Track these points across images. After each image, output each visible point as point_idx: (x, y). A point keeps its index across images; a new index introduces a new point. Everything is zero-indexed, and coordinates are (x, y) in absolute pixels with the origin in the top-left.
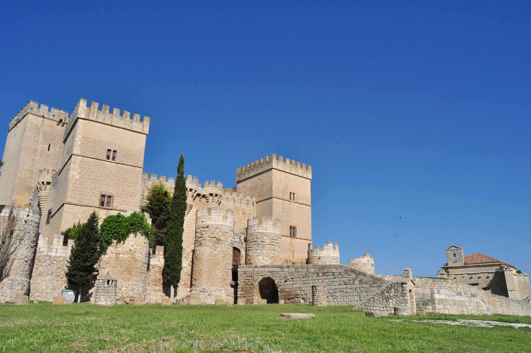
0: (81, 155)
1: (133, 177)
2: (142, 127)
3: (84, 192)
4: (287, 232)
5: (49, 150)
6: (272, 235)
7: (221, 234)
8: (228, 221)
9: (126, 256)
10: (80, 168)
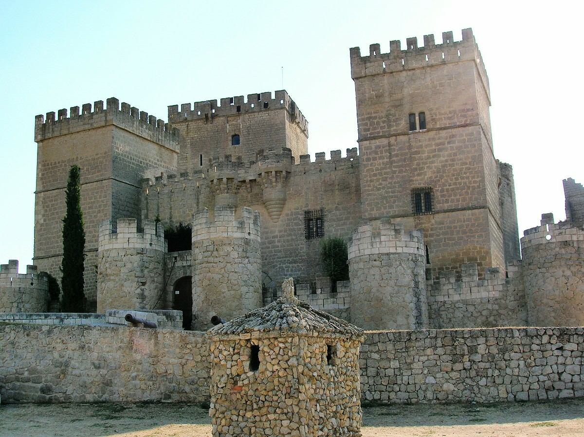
0: (44, 189)
1: (100, 196)
2: (104, 118)
3: (49, 238)
5: (201, 165)
7: (107, 265)
10: (44, 207)
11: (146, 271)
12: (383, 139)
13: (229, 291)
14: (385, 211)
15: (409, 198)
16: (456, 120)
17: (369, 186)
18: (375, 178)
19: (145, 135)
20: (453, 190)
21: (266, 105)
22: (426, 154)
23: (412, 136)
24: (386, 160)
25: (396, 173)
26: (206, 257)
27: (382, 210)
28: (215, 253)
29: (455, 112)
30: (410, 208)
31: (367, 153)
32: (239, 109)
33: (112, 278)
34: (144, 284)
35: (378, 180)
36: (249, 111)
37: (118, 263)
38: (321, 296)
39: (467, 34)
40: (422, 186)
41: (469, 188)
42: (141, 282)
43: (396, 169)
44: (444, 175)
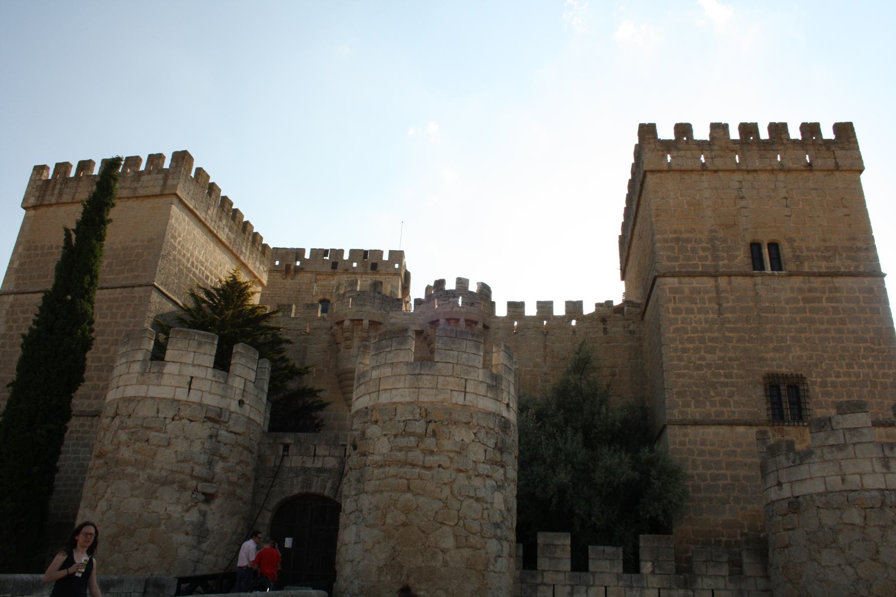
2: (161, 182)
4: (756, 403)
6: (403, 414)
7: (123, 436)
8: (166, 380)
11: (219, 467)
12: (705, 279)
13: (458, 548)
14: (713, 410)
15: (760, 391)
16: (838, 262)
17: (680, 359)
18: (691, 346)
19: (223, 236)
20: (843, 385)
21: (374, 267)
22: (788, 315)
23: (759, 280)
24: (711, 316)
25: (732, 342)
26: (400, 450)
27: (708, 407)
28: (430, 442)
29: (835, 249)
30: (763, 411)
31: (674, 298)
32: (334, 265)
33: (130, 470)
34: (209, 498)
35: (697, 350)
36: (348, 270)
37: (152, 434)
38: (654, 581)
39: (845, 131)
40: (784, 370)
41: (874, 385)
42: (203, 494)
43: (731, 335)
44: (826, 355)
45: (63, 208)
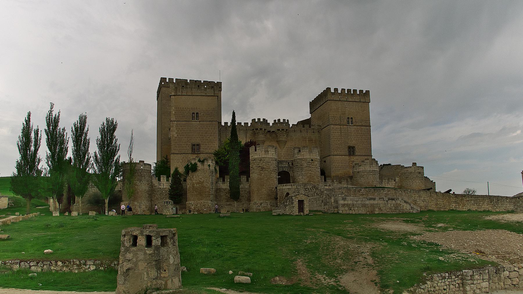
4: (346, 151)
9: (198, 185)
45: (183, 97)
